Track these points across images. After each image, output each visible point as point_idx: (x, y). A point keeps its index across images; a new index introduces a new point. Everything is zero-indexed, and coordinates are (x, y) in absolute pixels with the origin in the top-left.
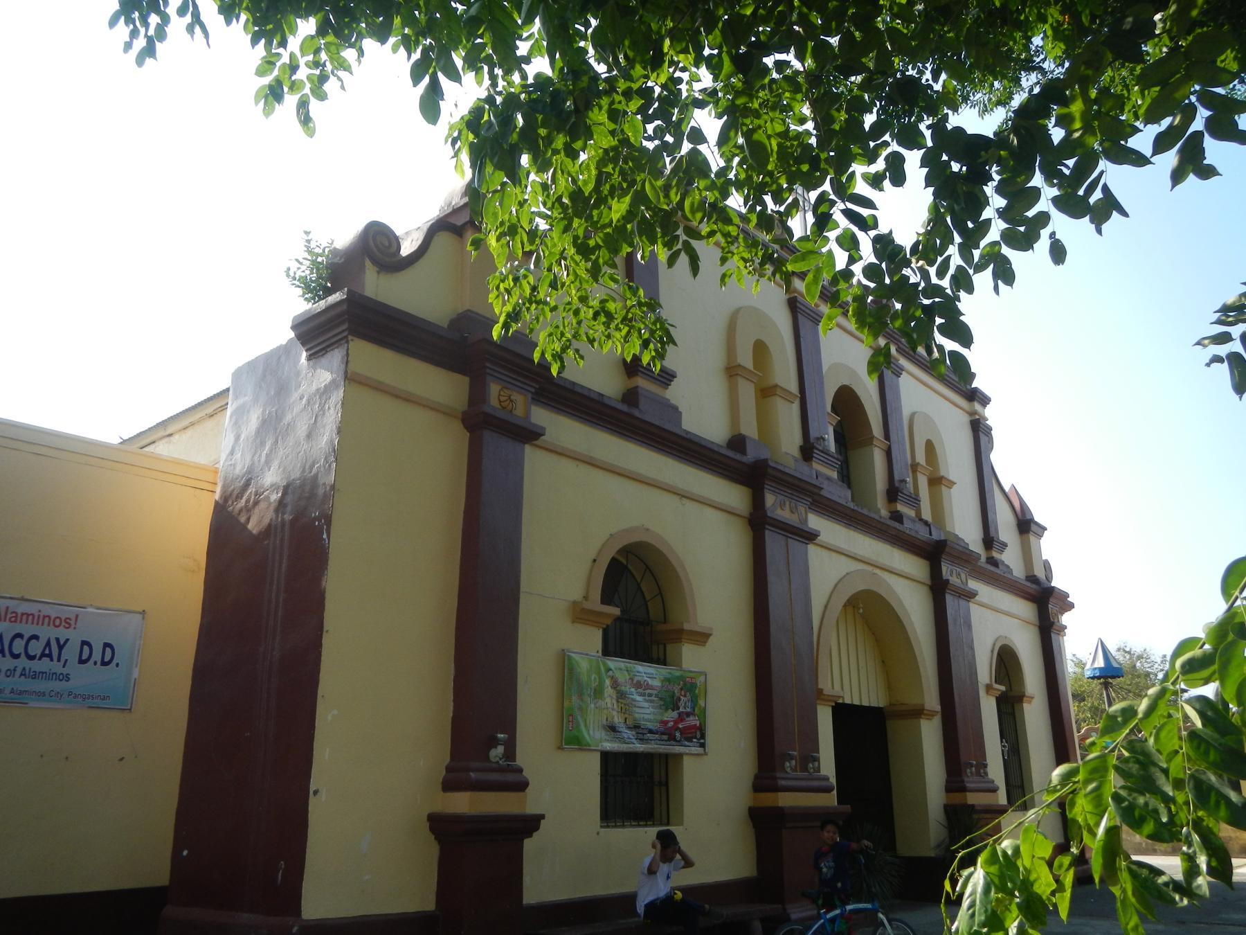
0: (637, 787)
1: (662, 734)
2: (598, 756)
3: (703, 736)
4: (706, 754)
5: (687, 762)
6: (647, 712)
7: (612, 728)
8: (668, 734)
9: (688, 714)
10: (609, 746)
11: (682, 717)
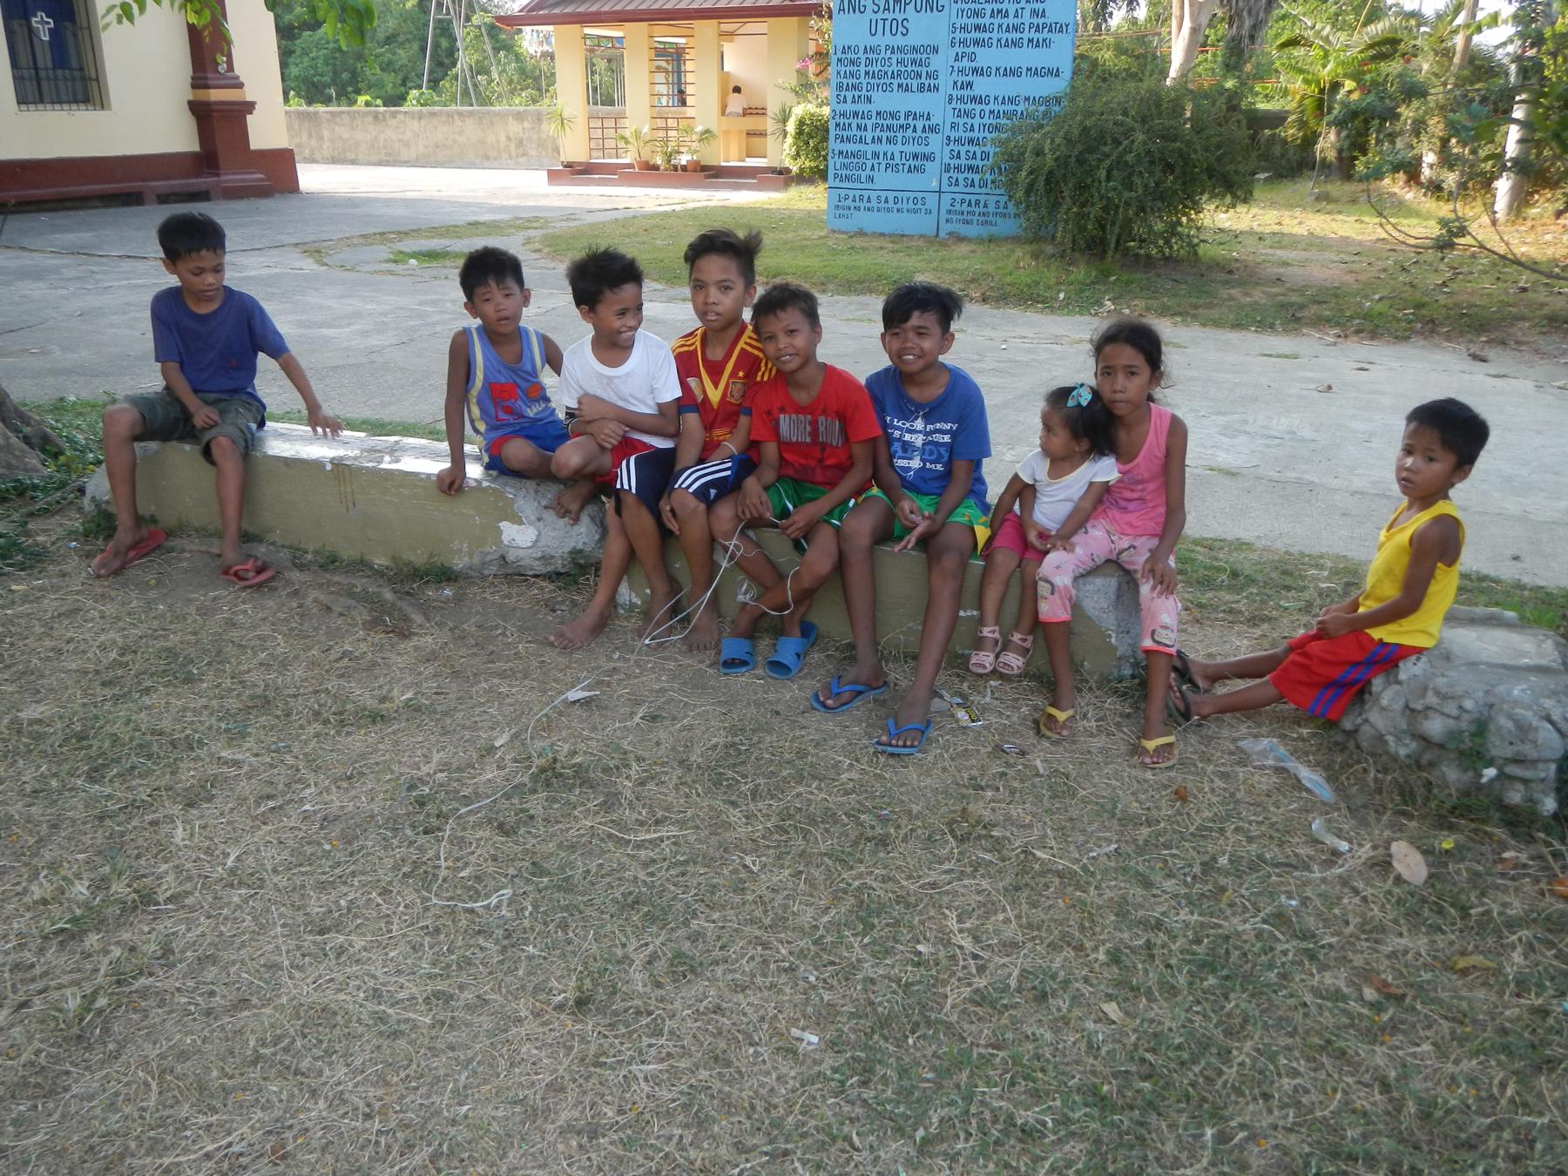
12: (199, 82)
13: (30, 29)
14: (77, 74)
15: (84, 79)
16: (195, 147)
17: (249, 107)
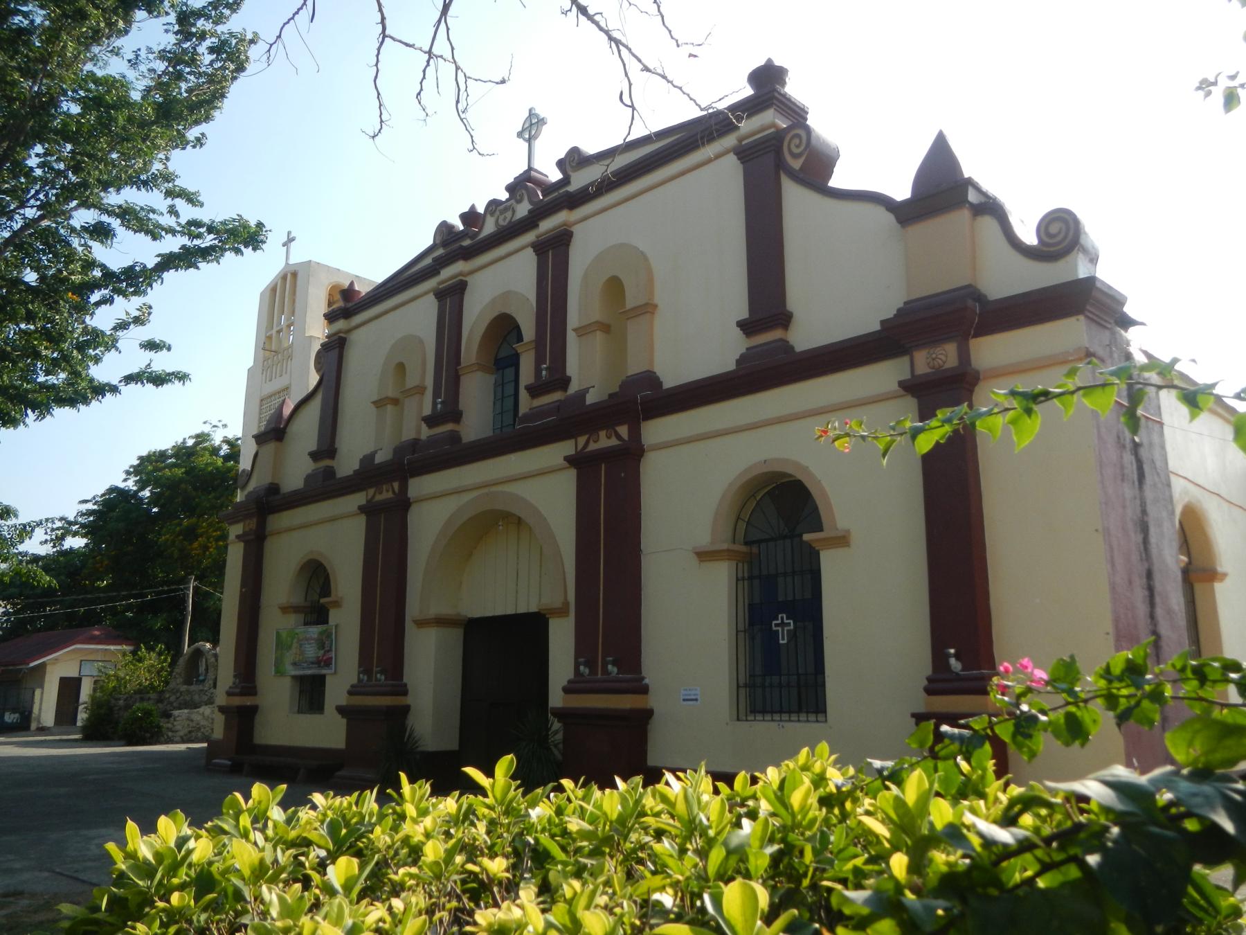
0: (311, 693)
5: (328, 679)
6: (311, 652)
10: (293, 673)
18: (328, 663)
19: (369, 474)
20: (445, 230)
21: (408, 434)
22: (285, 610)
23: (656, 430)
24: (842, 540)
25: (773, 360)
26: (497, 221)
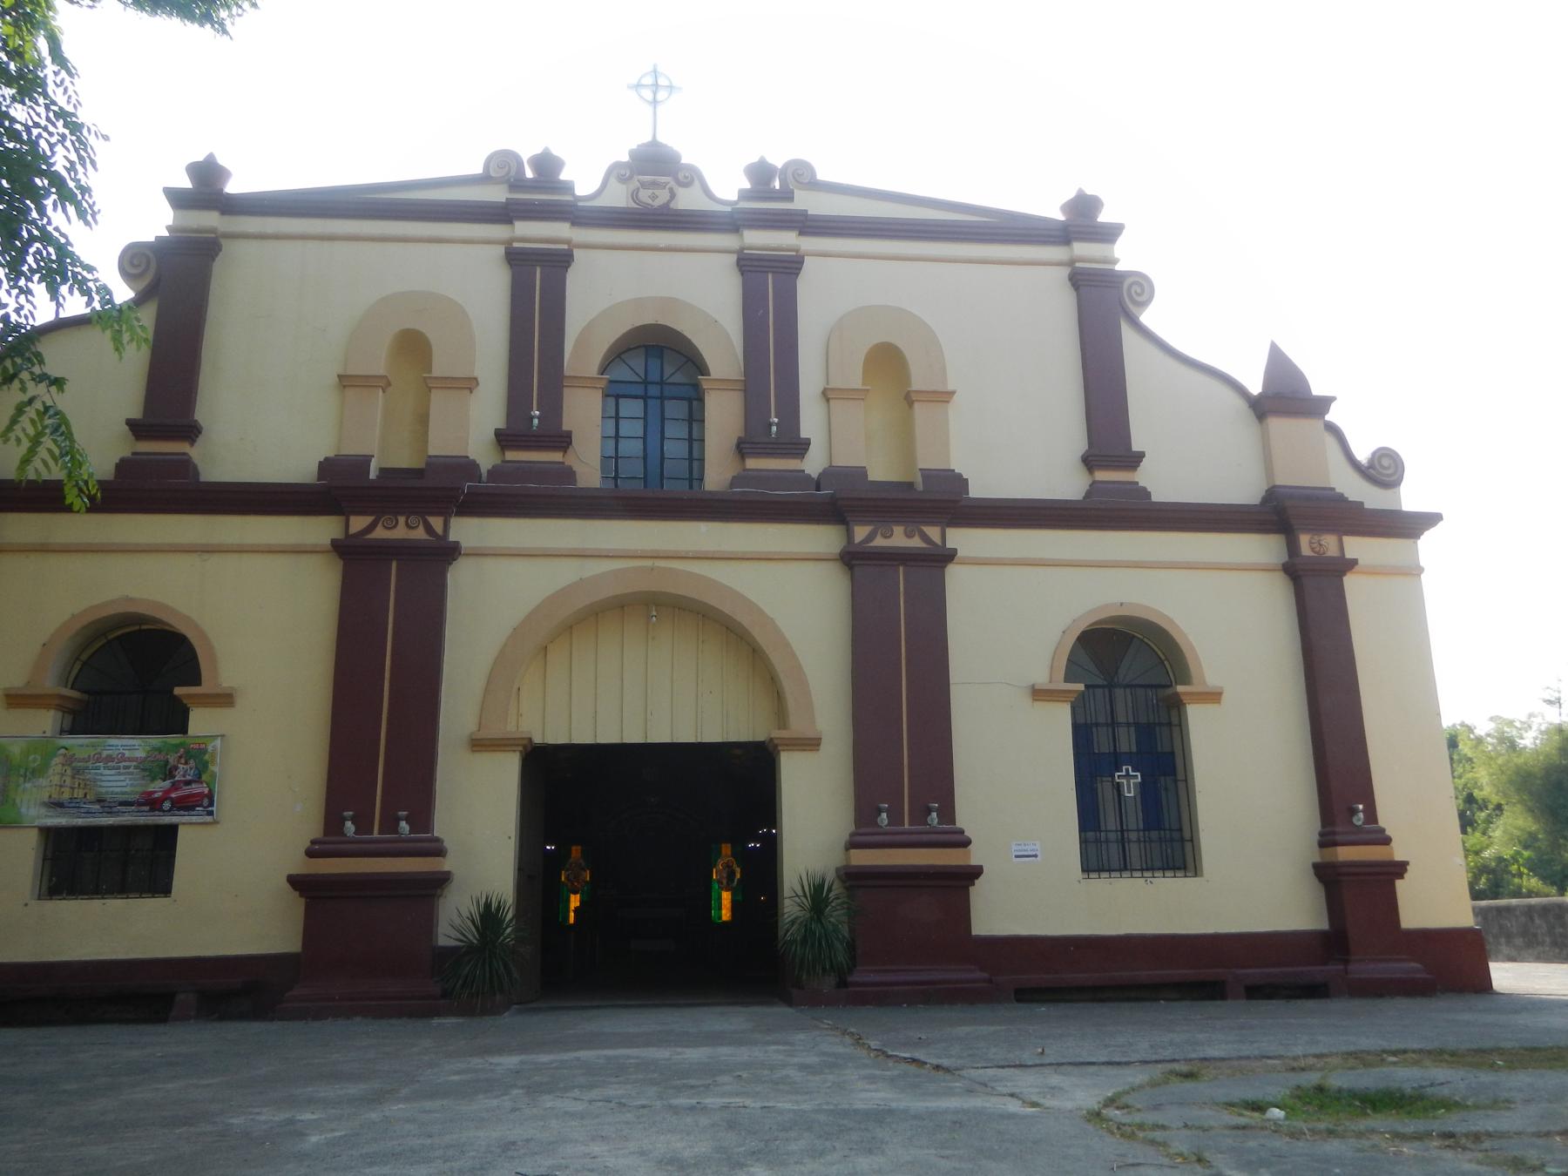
0: (113, 857)
1: (140, 804)
2: (34, 834)
3: (211, 804)
4: (216, 822)
5: (184, 835)
7: (60, 805)
8: (153, 804)
9: (188, 783)
11: (175, 787)
12: (1327, 840)
13: (1118, 787)
14: (1176, 835)
15: (1182, 840)
16: (1322, 924)
17: (1399, 869)
18: (199, 802)
19: (337, 489)
20: (503, 167)
21: (441, 444)
22: (18, 700)
23: (962, 539)
24: (1214, 697)
25: (1113, 500)
26: (634, 196)
